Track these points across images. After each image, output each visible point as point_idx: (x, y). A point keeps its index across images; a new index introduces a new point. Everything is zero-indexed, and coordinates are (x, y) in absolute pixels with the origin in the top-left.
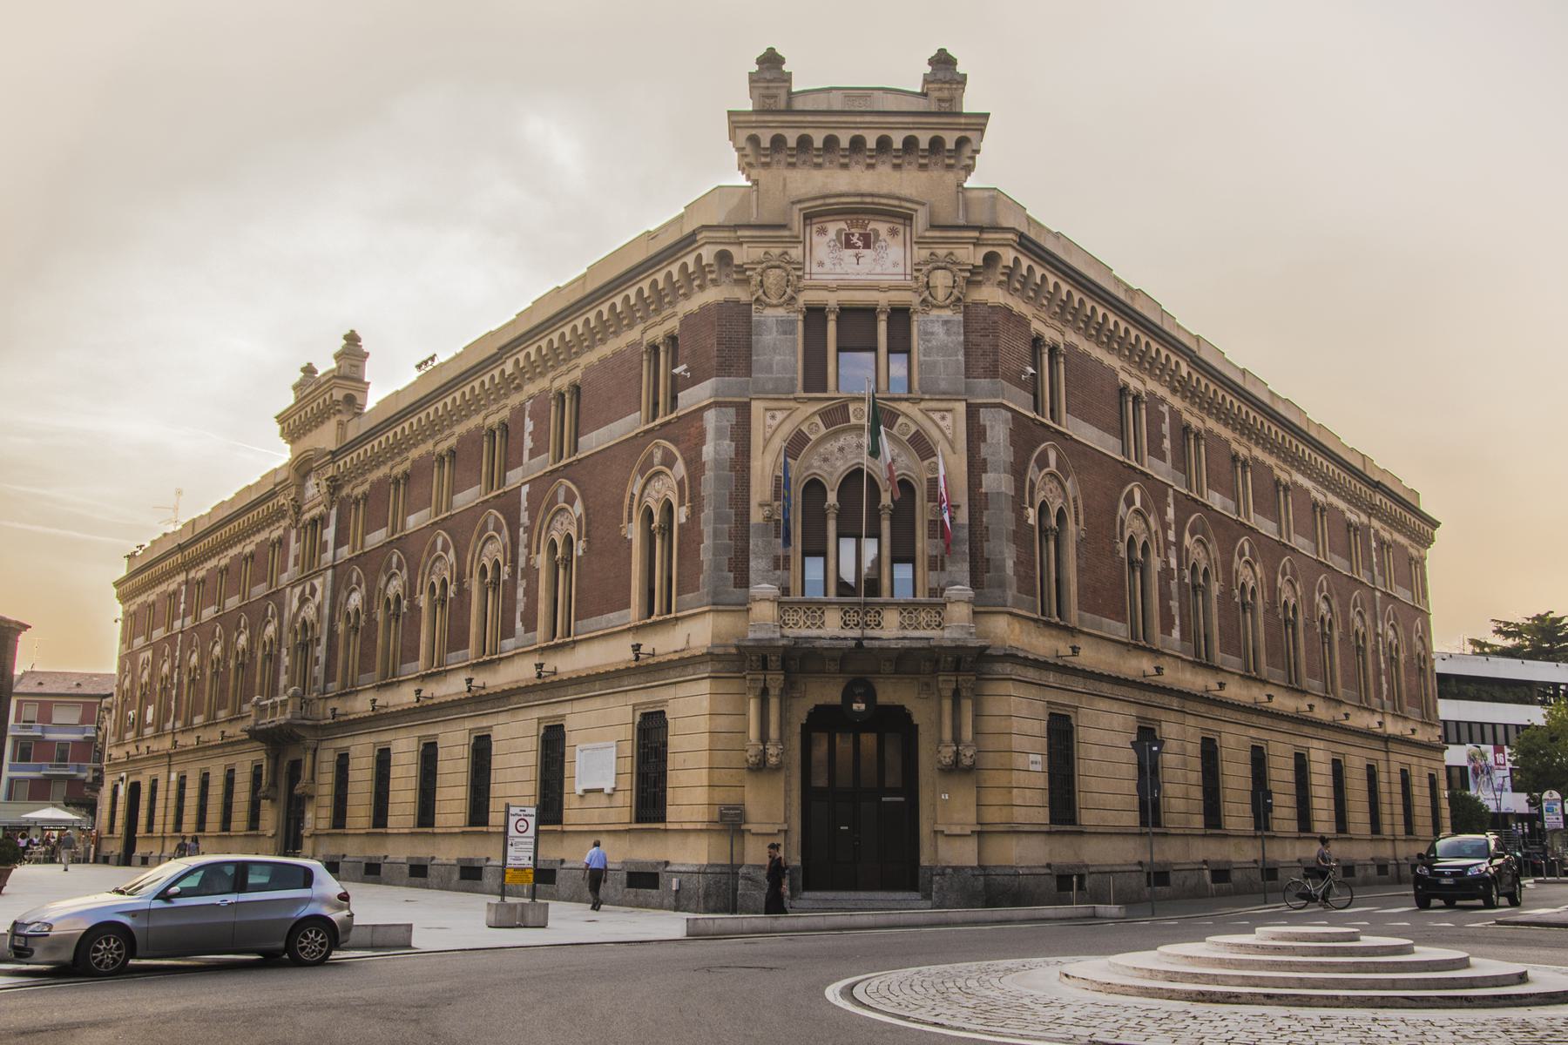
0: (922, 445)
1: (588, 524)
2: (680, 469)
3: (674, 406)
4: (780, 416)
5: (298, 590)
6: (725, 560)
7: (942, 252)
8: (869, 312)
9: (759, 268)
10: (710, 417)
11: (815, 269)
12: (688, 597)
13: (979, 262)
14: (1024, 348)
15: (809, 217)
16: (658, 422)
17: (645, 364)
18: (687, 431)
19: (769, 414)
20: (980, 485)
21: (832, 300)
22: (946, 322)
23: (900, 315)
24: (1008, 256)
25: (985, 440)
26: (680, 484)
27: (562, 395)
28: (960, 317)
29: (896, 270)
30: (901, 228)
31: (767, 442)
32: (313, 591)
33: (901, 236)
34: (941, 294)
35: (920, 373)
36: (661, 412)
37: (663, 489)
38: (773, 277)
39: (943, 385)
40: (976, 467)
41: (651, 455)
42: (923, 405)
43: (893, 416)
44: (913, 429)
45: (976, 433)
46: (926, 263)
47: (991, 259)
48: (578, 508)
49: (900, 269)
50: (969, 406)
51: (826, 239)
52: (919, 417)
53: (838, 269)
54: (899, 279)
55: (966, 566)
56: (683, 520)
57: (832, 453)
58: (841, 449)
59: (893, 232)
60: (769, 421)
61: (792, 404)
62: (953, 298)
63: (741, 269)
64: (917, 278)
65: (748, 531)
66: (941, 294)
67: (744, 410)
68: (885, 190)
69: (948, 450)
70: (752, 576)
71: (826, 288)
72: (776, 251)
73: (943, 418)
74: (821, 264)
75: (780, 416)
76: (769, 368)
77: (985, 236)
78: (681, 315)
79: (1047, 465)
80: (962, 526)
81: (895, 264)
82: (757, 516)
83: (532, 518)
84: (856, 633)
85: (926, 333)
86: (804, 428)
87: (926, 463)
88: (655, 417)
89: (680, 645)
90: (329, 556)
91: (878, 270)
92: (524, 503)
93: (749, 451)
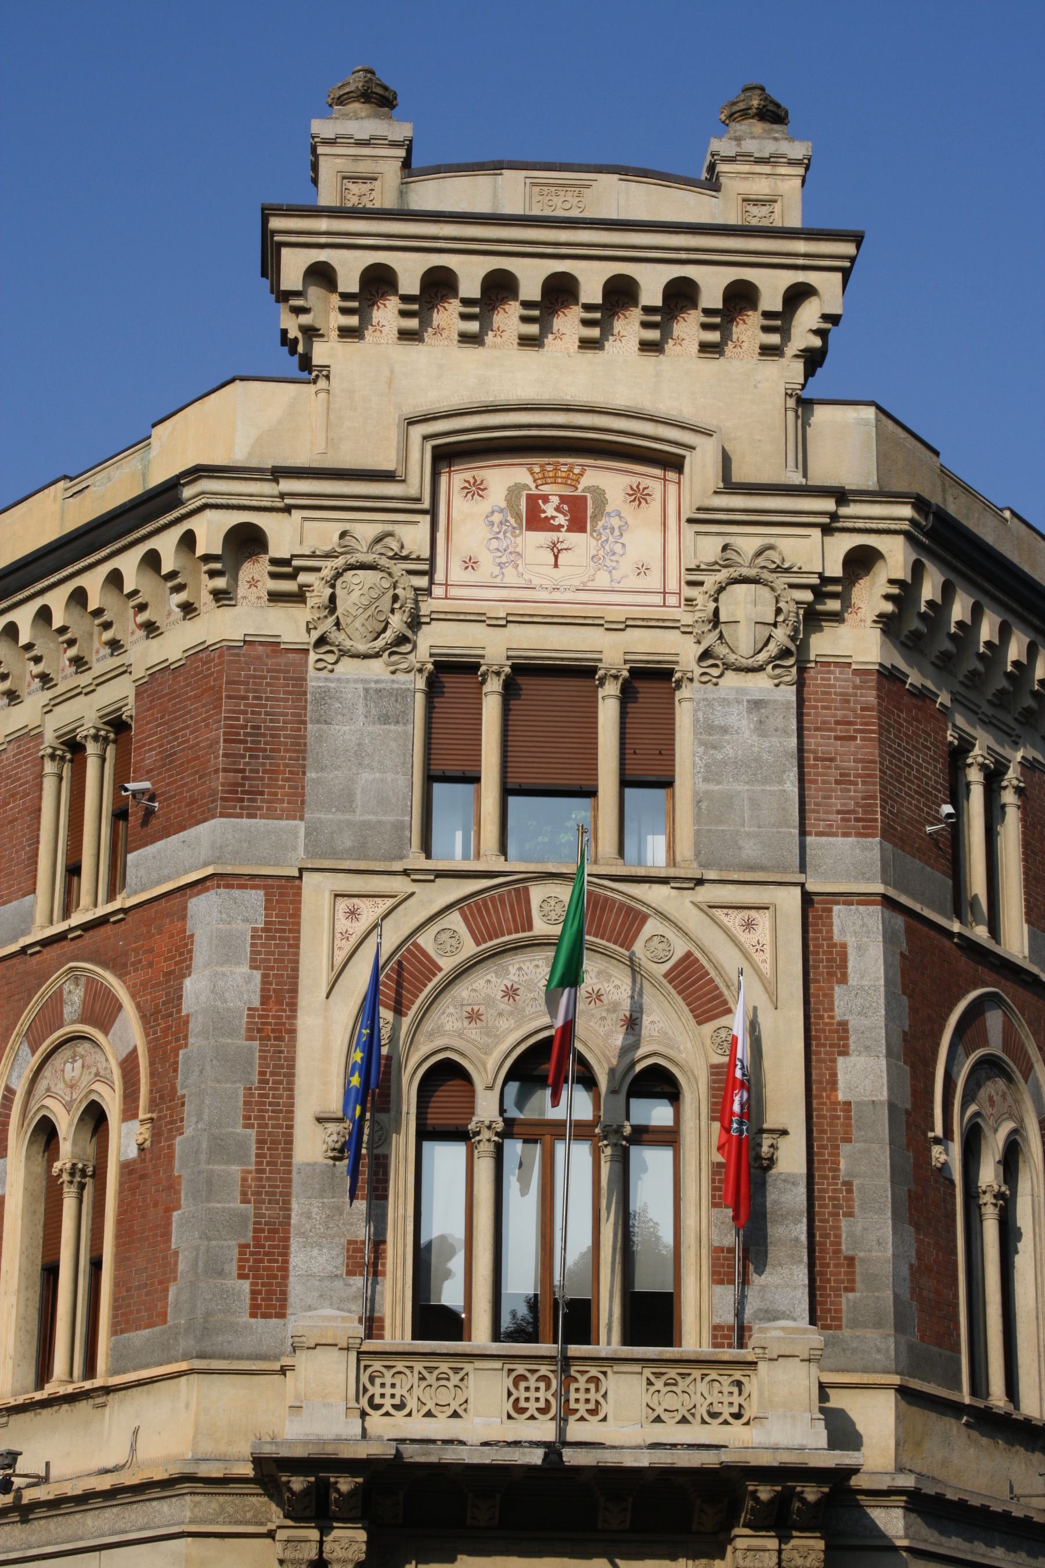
0: (697, 988)
2: (130, 1030)
3: (116, 883)
6: (230, 1250)
7: (748, 543)
8: (583, 672)
9: (328, 568)
10: (205, 912)
11: (457, 574)
12: (140, 1336)
13: (835, 569)
14: (935, 774)
15: (446, 456)
16: (78, 918)
17: (49, 785)
18: (148, 943)
19: (343, 904)
20: (833, 1083)
21: (495, 648)
22: (757, 705)
24: (896, 557)
25: (844, 980)
26: (129, 1065)
28: (789, 694)
29: (641, 583)
30: (655, 487)
34: (743, 641)
35: (698, 818)
36: (85, 899)
38: (357, 591)
39: (750, 850)
40: (822, 1040)
41: (58, 999)
42: (706, 894)
43: (633, 919)
44: (680, 948)
45: (820, 964)
46: (712, 568)
47: (861, 561)
49: (654, 581)
50: (807, 899)
51: (482, 507)
53: (510, 577)
54: (649, 605)
55: (801, 1275)
56: (133, 1153)
57: (489, 1001)
59: (638, 496)
61: (400, 885)
62: (773, 649)
64: (689, 601)
65: (287, 1182)
66: (743, 641)
67: (283, 894)
68: (621, 399)
69: (762, 1001)
70: (295, 1288)
71: (478, 618)
72: (366, 530)
73: (749, 925)
74: (470, 564)
75: (370, 911)
76: (346, 800)
78: (139, 672)
79: (985, 1043)
80: (790, 1180)
81: (642, 570)
84: (545, 1430)
85: (710, 728)
86: (426, 940)
87: (709, 1028)
88: (66, 914)
91: (603, 580)
93: (294, 991)
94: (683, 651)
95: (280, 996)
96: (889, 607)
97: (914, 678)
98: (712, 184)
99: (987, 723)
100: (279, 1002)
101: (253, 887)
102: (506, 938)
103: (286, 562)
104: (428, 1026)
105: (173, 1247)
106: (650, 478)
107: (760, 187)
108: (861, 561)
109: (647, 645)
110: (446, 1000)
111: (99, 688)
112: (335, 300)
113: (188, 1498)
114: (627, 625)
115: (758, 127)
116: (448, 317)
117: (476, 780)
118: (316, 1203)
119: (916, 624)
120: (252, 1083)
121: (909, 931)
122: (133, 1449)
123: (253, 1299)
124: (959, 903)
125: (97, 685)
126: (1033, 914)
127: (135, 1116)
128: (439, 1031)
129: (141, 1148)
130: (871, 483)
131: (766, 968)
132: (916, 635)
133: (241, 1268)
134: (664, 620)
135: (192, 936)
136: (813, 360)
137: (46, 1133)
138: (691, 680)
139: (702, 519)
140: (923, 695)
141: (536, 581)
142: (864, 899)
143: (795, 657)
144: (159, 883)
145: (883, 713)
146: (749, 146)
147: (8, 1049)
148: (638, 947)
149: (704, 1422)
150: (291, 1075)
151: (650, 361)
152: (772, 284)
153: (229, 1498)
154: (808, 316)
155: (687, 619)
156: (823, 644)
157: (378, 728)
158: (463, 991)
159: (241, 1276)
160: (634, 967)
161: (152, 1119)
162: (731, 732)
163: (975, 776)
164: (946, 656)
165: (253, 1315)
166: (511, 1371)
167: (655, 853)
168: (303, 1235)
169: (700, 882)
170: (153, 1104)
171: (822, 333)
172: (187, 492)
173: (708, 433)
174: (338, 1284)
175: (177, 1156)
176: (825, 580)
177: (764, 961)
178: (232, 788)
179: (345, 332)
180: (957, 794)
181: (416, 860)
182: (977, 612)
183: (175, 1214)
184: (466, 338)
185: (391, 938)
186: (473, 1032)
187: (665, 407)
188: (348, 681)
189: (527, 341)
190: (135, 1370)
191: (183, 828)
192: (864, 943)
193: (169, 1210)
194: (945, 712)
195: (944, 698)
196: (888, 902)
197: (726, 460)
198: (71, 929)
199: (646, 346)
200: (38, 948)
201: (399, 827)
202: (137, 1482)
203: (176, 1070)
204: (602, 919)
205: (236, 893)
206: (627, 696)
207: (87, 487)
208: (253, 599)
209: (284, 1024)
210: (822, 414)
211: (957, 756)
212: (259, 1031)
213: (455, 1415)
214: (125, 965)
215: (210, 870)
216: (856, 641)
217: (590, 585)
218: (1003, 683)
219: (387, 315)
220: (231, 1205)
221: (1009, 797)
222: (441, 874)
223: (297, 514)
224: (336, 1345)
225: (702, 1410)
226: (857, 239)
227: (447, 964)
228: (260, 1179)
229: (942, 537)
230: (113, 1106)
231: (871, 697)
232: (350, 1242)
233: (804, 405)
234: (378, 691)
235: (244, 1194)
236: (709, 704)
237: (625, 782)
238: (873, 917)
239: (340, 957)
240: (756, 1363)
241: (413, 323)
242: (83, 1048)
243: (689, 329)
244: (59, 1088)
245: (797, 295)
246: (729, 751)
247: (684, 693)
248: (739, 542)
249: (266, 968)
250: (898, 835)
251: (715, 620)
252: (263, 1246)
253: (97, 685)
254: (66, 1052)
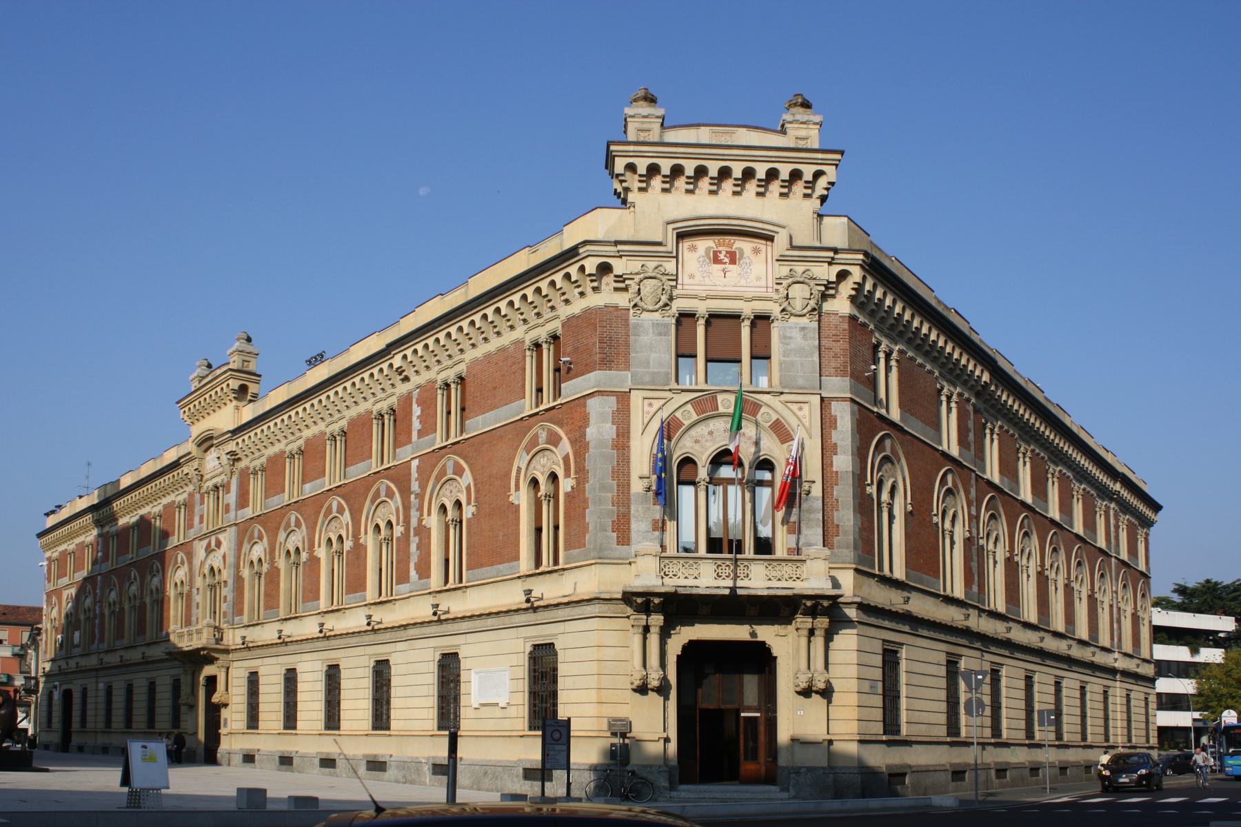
0: (781, 431)
1: (477, 491)
2: (566, 446)
3: (557, 393)
4: (657, 404)
5: (205, 543)
7: (799, 268)
8: (736, 317)
13: (833, 279)
14: (868, 353)
18: (572, 416)
19: (646, 402)
22: (803, 329)
23: (761, 321)
24: (857, 274)
26: (566, 459)
27: (448, 385)
29: (758, 284)
30: (763, 248)
32: (219, 544)
33: (763, 254)
34: (798, 306)
35: (781, 370)
37: (554, 460)
39: (801, 382)
42: (783, 398)
43: (756, 407)
44: (774, 417)
45: (827, 423)
46: (786, 278)
47: (843, 275)
48: (467, 478)
49: (763, 283)
50: (822, 399)
52: (779, 407)
54: (761, 292)
56: (569, 489)
57: (702, 436)
58: (711, 433)
59: (756, 251)
60: (647, 408)
61: (668, 395)
62: (809, 308)
63: (620, 278)
66: (798, 306)
67: (623, 398)
68: (749, 214)
73: (800, 409)
75: (657, 404)
81: (758, 279)
82: (637, 487)
83: (423, 487)
85: (785, 337)
86: (678, 414)
90: (232, 514)
91: (743, 282)
92: (414, 475)
93: (629, 432)
94: (774, 309)
95: (623, 434)
96: (853, 293)
97: (862, 319)
98: (783, 131)
99: (887, 336)
104: (680, 445)
106: (760, 244)
107: (802, 133)
108: (843, 275)
109: (761, 307)
110: (686, 436)
112: (637, 177)
114: (753, 299)
115: (801, 110)
116: (681, 183)
117: (695, 356)
119: (863, 299)
121: (859, 411)
124: (876, 401)
126: (901, 405)
128: (684, 446)
130: (846, 246)
131: (807, 424)
132: (863, 303)
136: (823, 199)
137: (535, 483)
139: (782, 259)
140: (864, 325)
142: (844, 399)
143: (817, 311)
145: (851, 332)
146: (798, 117)
148: (759, 417)
150: (629, 462)
151: (760, 199)
152: (808, 171)
154: (822, 183)
155: (776, 297)
156: (828, 306)
158: (693, 432)
160: (757, 424)
162: (793, 339)
163: (882, 355)
164: (873, 311)
167: (763, 383)
170: (576, 472)
171: (827, 189)
173: (783, 227)
176: (829, 283)
177: (806, 422)
179: (641, 189)
180: (876, 361)
181: (674, 385)
182: (885, 294)
184: (688, 191)
185: (665, 414)
186: (697, 447)
187: (766, 217)
189: (712, 192)
192: (844, 416)
194: (872, 331)
195: (872, 327)
196: (852, 400)
197: (791, 238)
199: (758, 194)
201: (667, 374)
204: (746, 408)
206: (753, 325)
210: (826, 220)
211: (876, 347)
216: (841, 305)
218: (893, 321)
219: (657, 182)
221: (893, 363)
222: (683, 391)
226: (842, 153)
227: (687, 423)
229: (874, 267)
230: (560, 473)
231: (846, 326)
233: (820, 216)
236: (785, 328)
237: (753, 357)
238: (847, 406)
239: (646, 421)
241: (667, 186)
242: (547, 453)
243: (775, 187)
244: (538, 467)
245: (818, 175)
246: (793, 346)
247: (775, 324)
248: (796, 268)
250: (856, 376)
251: (787, 297)
254: (541, 454)
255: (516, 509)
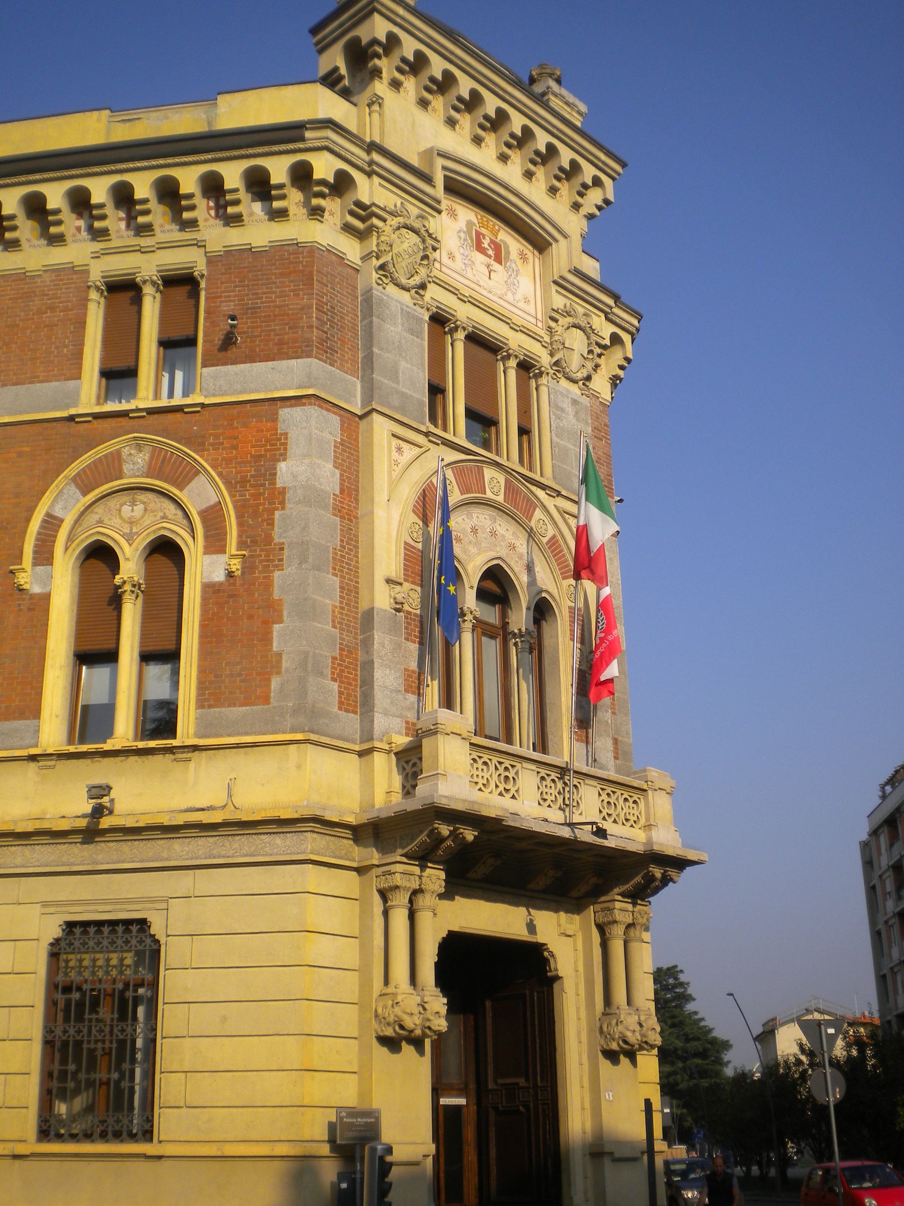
4: (410, 452)
11: (445, 260)
21: (463, 313)
31: (394, 485)
54: (529, 322)
60: (395, 455)
77: (616, 310)
89: (217, 797)
100: (350, 495)
101: (334, 413)
102: (477, 495)
103: (363, 207)
105: (275, 649)
111: (158, 251)
113: (309, 835)
118: (388, 637)
120: (336, 545)
122: (230, 796)
123: (340, 697)
125: (158, 248)
127: (222, 551)
129: (230, 574)
133: (333, 673)
134: (537, 334)
135: (286, 434)
138: (548, 374)
141: (481, 283)
144: (241, 392)
147: (54, 485)
149: (623, 824)
153: (333, 838)
157: (408, 336)
159: (334, 680)
161: (244, 556)
165: (340, 709)
166: (538, 772)
168: (381, 657)
169: (559, 494)
170: (241, 545)
171: (599, 208)
172: (308, 134)
174: (400, 697)
175: (275, 584)
178: (322, 341)
183: (276, 627)
188: (392, 299)
190: (229, 735)
191: (273, 360)
193: (267, 624)
198: (138, 410)
200: (90, 419)
202: (260, 818)
203: (272, 524)
205: (325, 413)
207: (138, 119)
208: (332, 223)
209: (352, 511)
212: (340, 511)
213: (513, 797)
214: (203, 444)
215: (310, 391)
217: (505, 297)
220: (326, 627)
223: (376, 179)
224: (460, 735)
225: (622, 816)
226: (624, 165)
228: (342, 614)
232: (406, 670)
234: (408, 313)
235: (333, 621)
240: (645, 790)
249: (342, 470)
252: (344, 661)
253: (158, 248)
255: (41, 604)
